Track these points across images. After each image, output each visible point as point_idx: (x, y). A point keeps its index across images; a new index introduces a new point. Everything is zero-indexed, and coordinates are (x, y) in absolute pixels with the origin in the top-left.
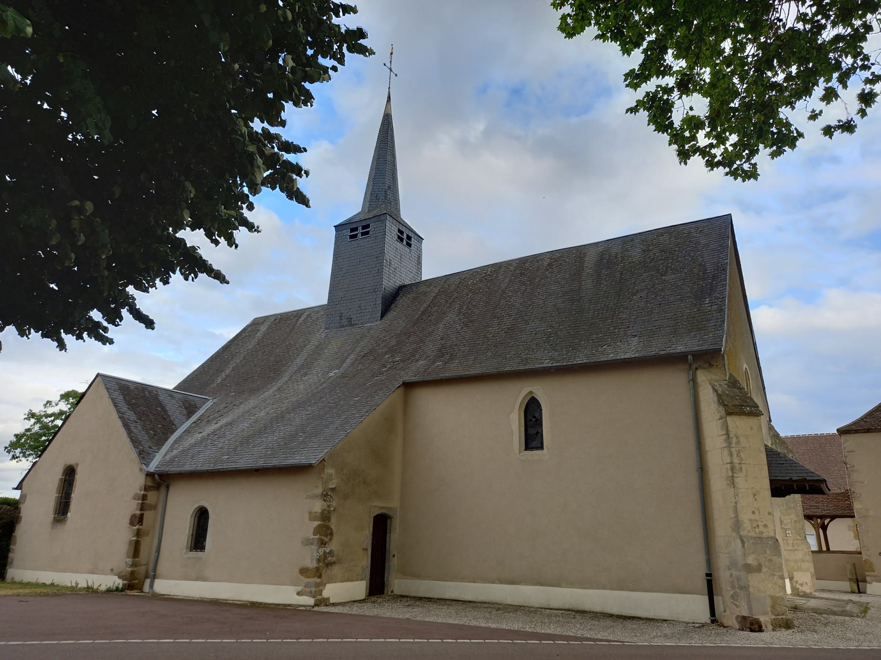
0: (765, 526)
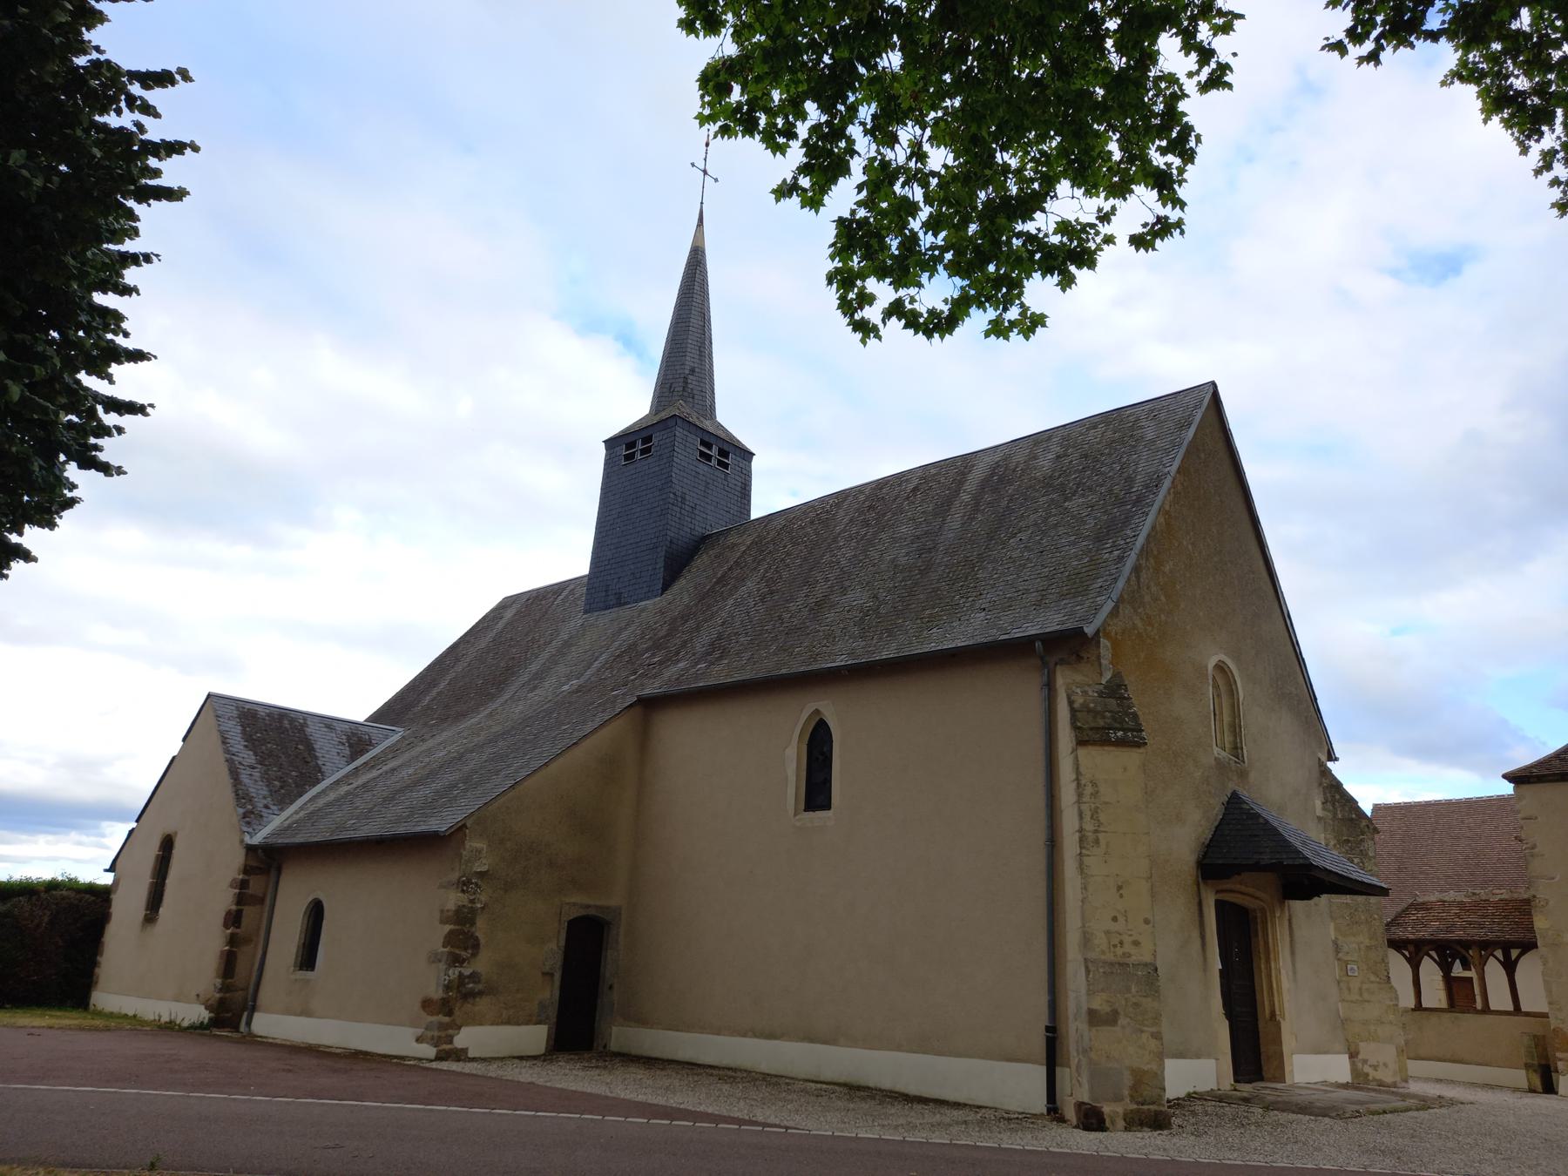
0: (1136, 943)
